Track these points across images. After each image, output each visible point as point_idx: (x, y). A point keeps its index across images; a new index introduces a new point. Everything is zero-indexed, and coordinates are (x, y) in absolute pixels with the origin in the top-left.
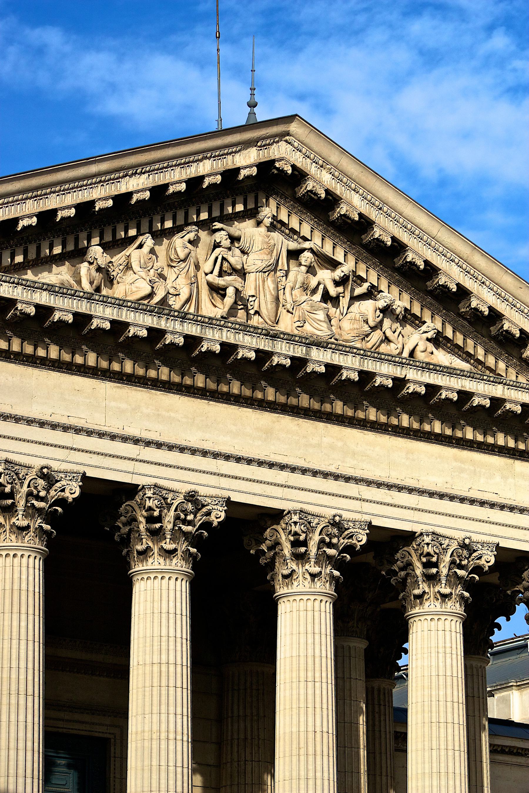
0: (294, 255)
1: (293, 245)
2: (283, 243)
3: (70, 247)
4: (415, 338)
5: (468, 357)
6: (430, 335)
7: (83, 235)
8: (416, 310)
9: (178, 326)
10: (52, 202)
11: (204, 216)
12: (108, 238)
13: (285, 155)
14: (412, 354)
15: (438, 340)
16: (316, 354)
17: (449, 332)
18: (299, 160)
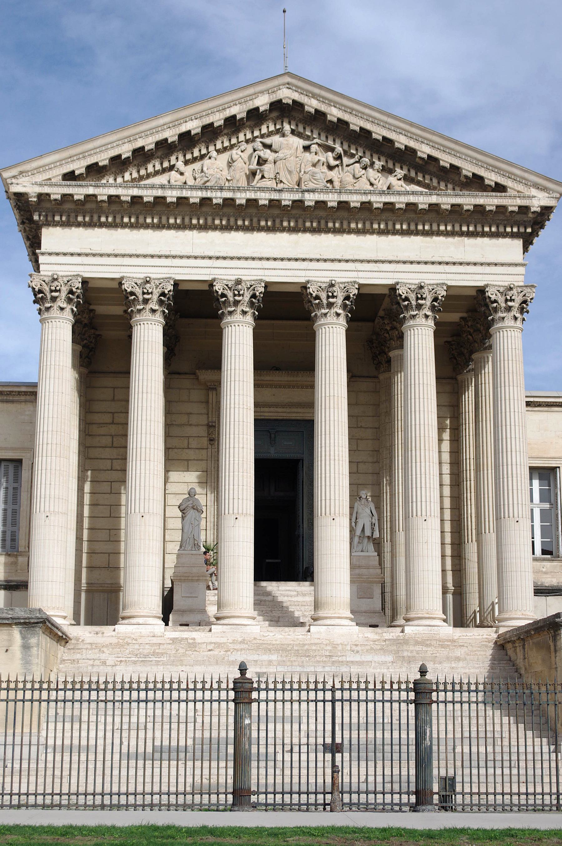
0: (307, 148)
1: (307, 143)
2: (300, 143)
3: (166, 164)
4: (392, 179)
5: (419, 183)
6: (399, 176)
7: (173, 158)
8: (390, 165)
9: (219, 194)
10: (139, 144)
11: (249, 136)
12: (189, 156)
13: (287, 95)
14: (389, 188)
15: (407, 179)
16: (307, 196)
17: (413, 174)
18: (296, 96)
